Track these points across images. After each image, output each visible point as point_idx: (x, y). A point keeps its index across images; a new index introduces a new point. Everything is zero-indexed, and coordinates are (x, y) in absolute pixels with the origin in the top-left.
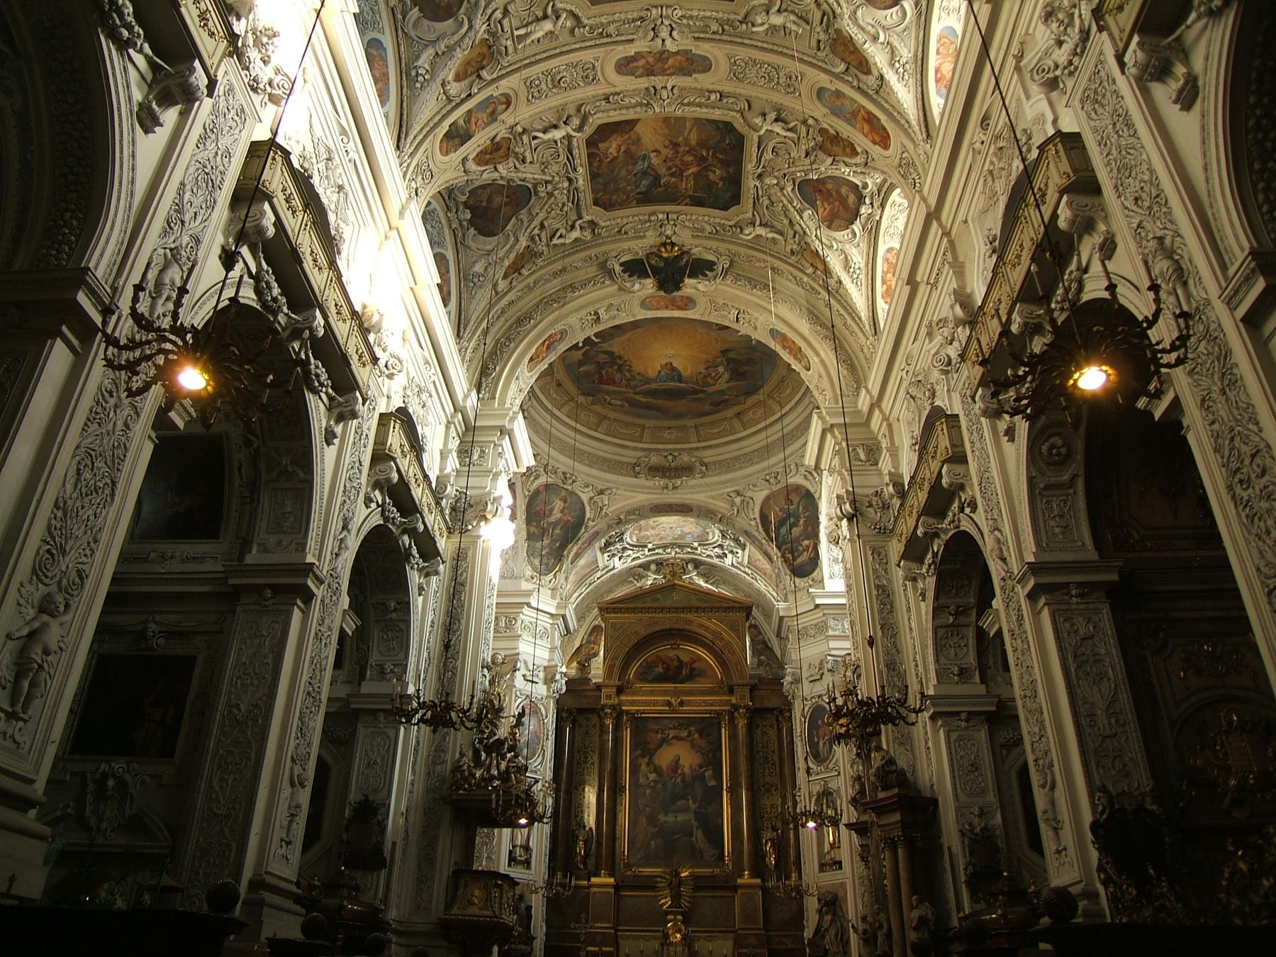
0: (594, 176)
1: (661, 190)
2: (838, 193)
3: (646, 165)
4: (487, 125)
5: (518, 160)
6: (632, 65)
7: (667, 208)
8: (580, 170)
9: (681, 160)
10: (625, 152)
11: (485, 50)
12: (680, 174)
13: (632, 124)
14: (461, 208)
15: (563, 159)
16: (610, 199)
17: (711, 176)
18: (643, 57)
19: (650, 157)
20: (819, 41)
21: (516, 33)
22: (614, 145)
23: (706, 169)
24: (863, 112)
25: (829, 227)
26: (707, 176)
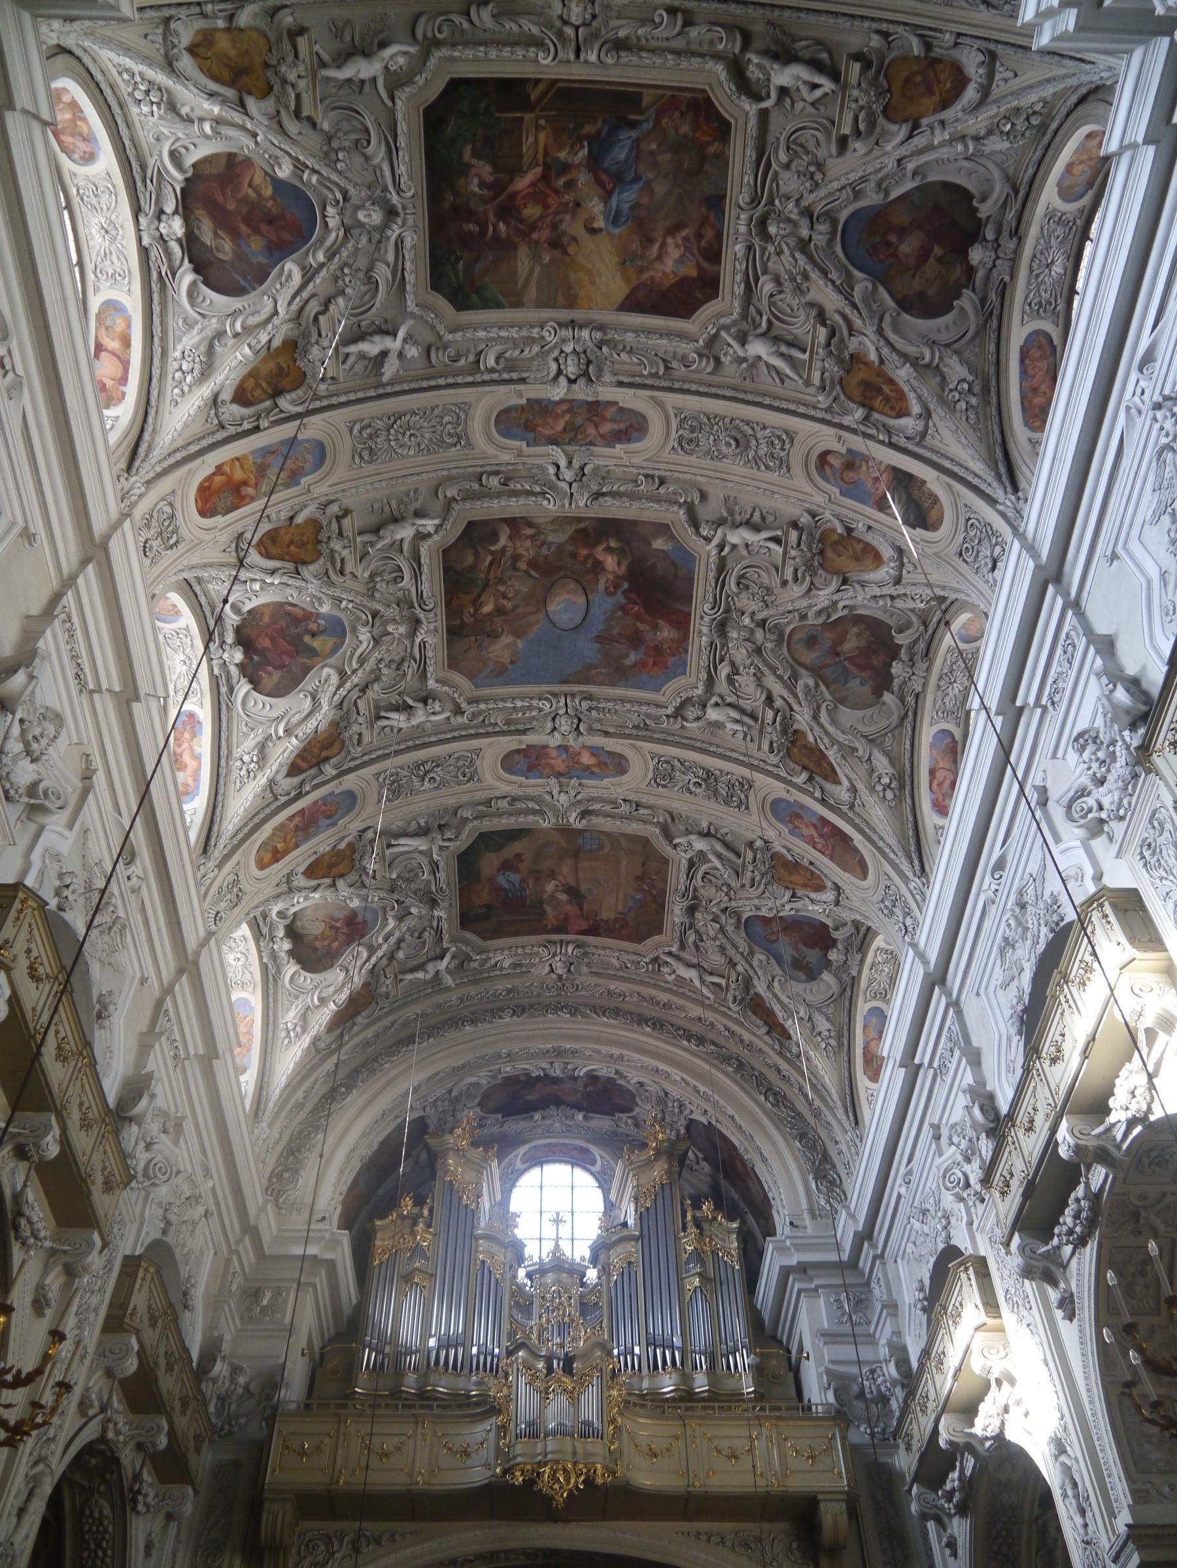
0: (716, 202)
1: (589, 129)
2: (235, 234)
3: (614, 200)
4: (865, 458)
5: (842, 340)
6: (622, 426)
7: (577, 72)
8: (739, 249)
9: (546, 207)
10: (650, 241)
11: (830, 554)
12: (553, 169)
13: (632, 304)
14: (980, 275)
15: (766, 286)
16: (696, 127)
17: (484, 170)
18: (602, 436)
19: (606, 218)
20: (340, 534)
21: (780, 550)
22: (669, 264)
23: (497, 187)
24: (250, 491)
25: (231, 156)
26: (496, 169)
